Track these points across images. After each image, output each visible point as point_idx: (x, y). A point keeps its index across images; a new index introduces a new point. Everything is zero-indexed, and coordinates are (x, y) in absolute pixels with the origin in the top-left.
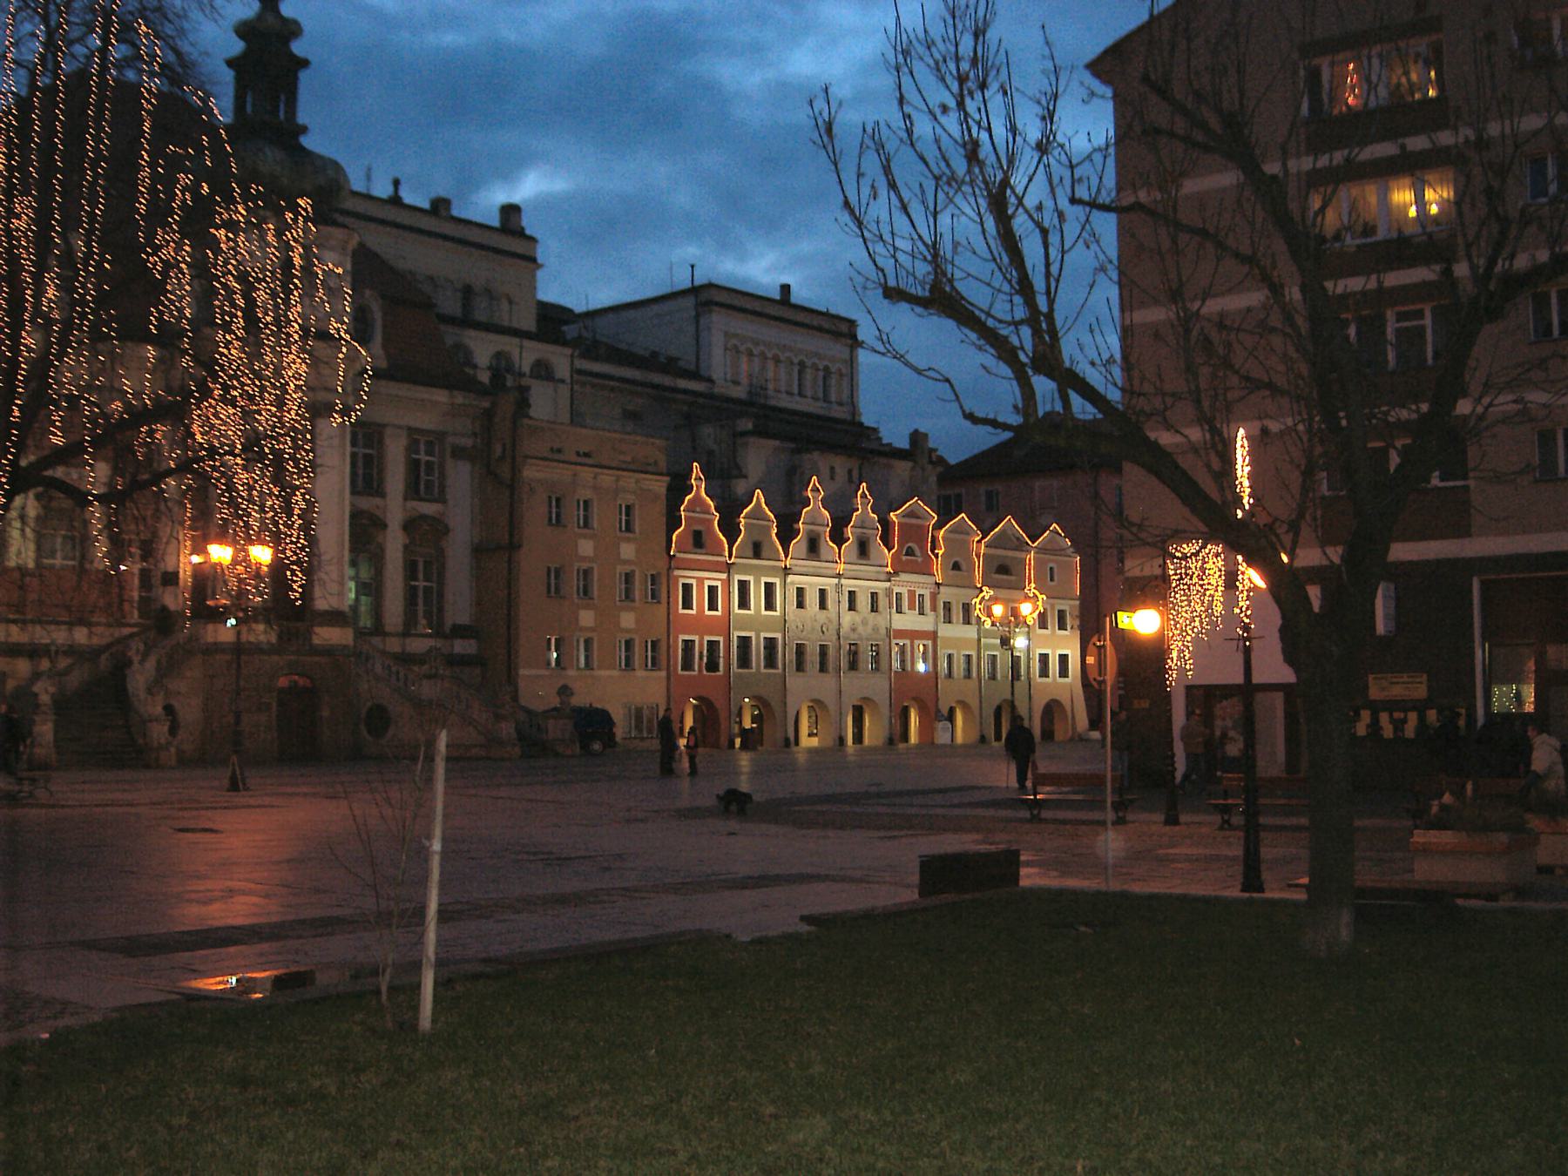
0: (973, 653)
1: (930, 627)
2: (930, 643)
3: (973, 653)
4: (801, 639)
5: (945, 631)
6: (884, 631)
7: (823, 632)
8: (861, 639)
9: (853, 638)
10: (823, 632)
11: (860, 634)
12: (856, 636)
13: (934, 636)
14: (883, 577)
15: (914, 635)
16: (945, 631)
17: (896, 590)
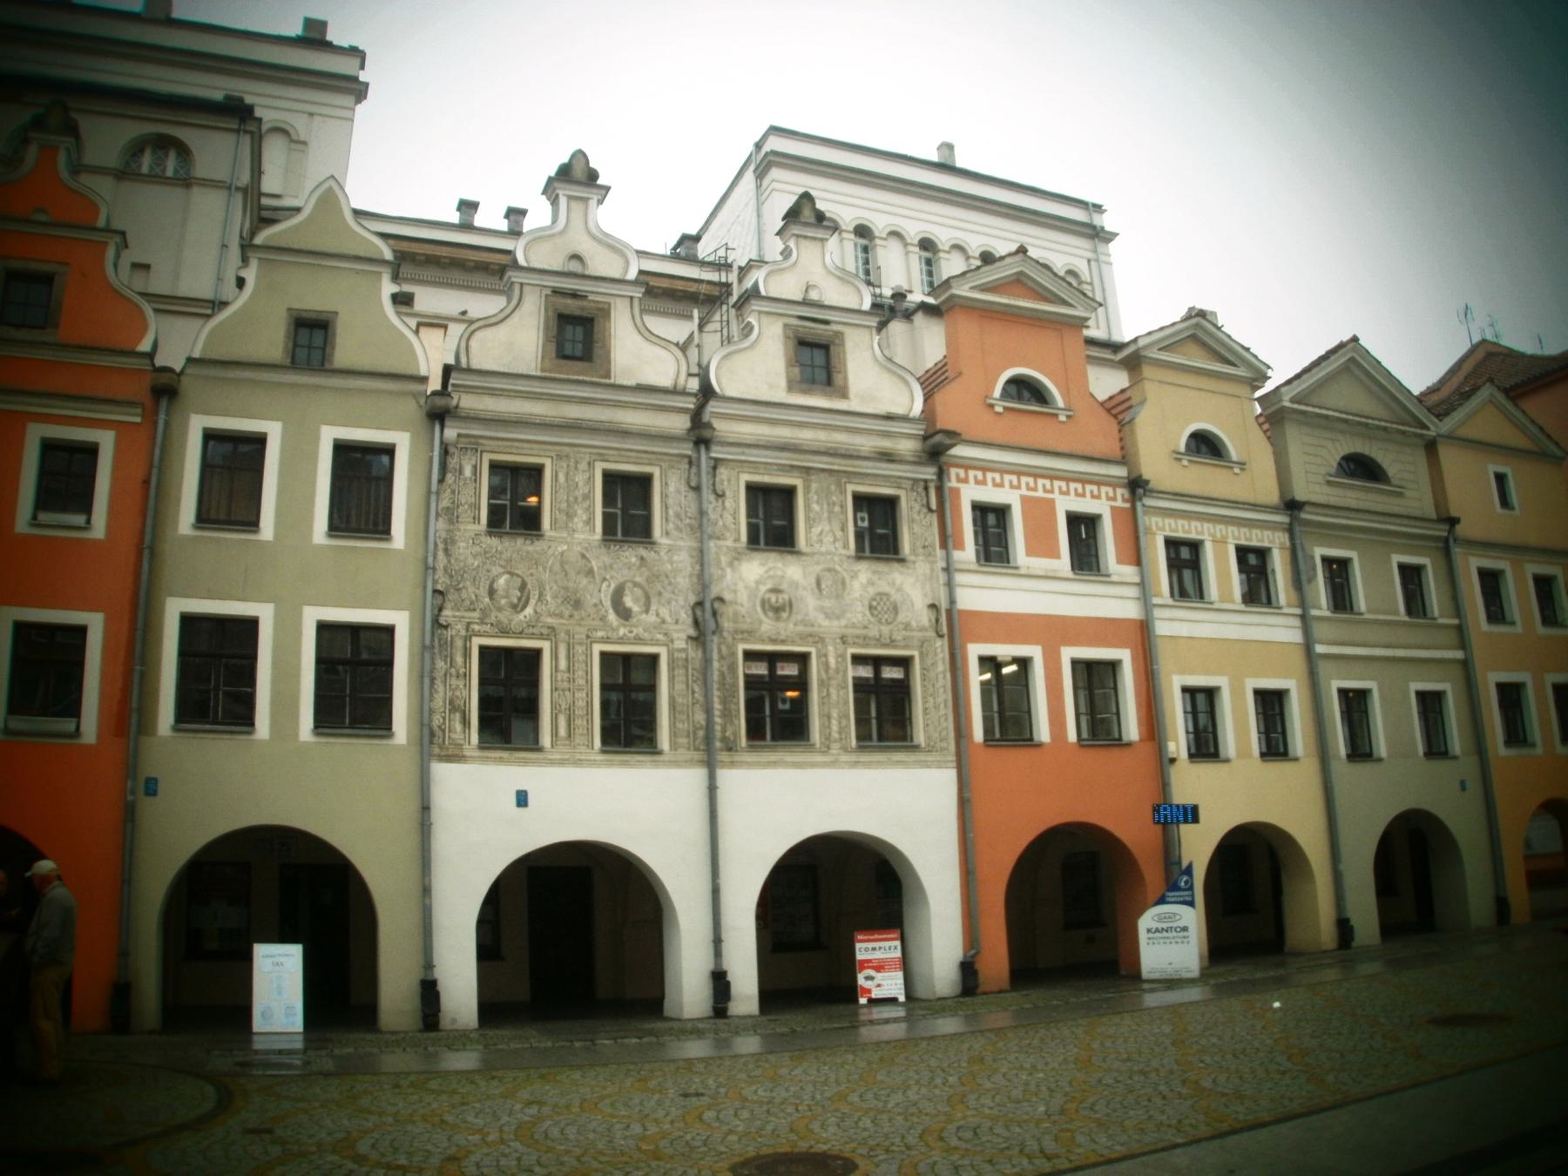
0: (1292, 685)
1: (1129, 610)
2: (1124, 655)
3: (1292, 685)
4: (505, 632)
5: (1174, 623)
6: (925, 618)
7: (625, 614)
8: (819, 640)
9: (771, 634)
10: (625, 614)
11: (804, 623)
12: (787, 627)
13: (1142, 635)
14: (907, 447)
15: (1054, 630)
16: (1174, 623)
17: (971, 492)
